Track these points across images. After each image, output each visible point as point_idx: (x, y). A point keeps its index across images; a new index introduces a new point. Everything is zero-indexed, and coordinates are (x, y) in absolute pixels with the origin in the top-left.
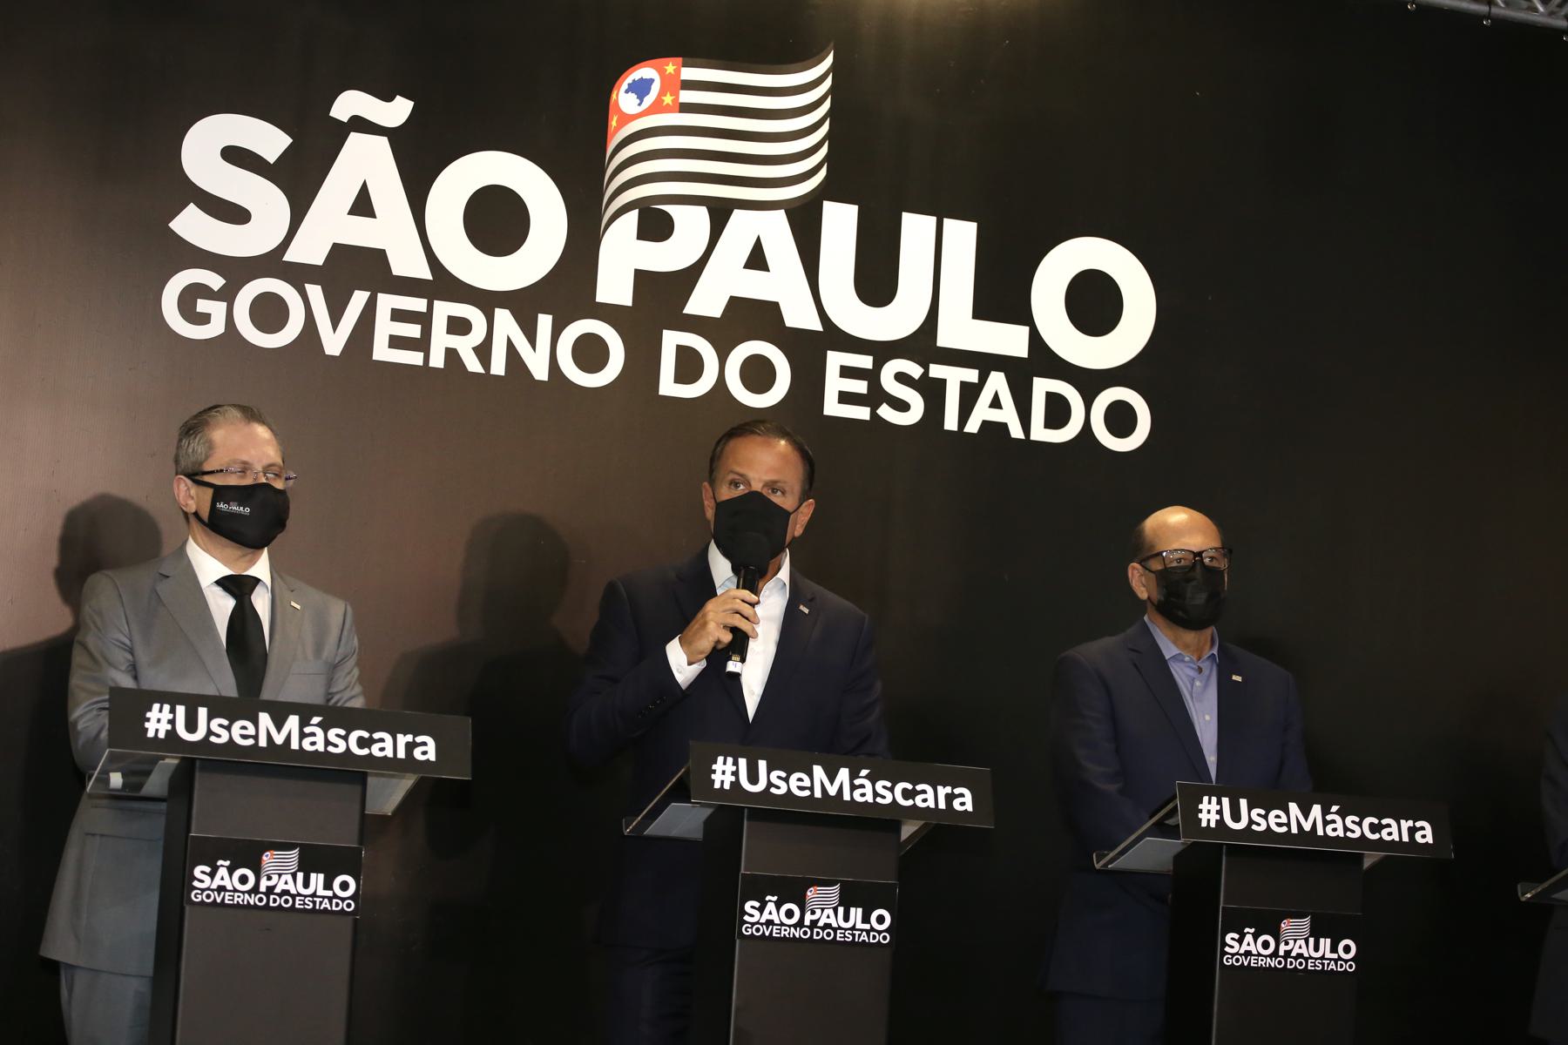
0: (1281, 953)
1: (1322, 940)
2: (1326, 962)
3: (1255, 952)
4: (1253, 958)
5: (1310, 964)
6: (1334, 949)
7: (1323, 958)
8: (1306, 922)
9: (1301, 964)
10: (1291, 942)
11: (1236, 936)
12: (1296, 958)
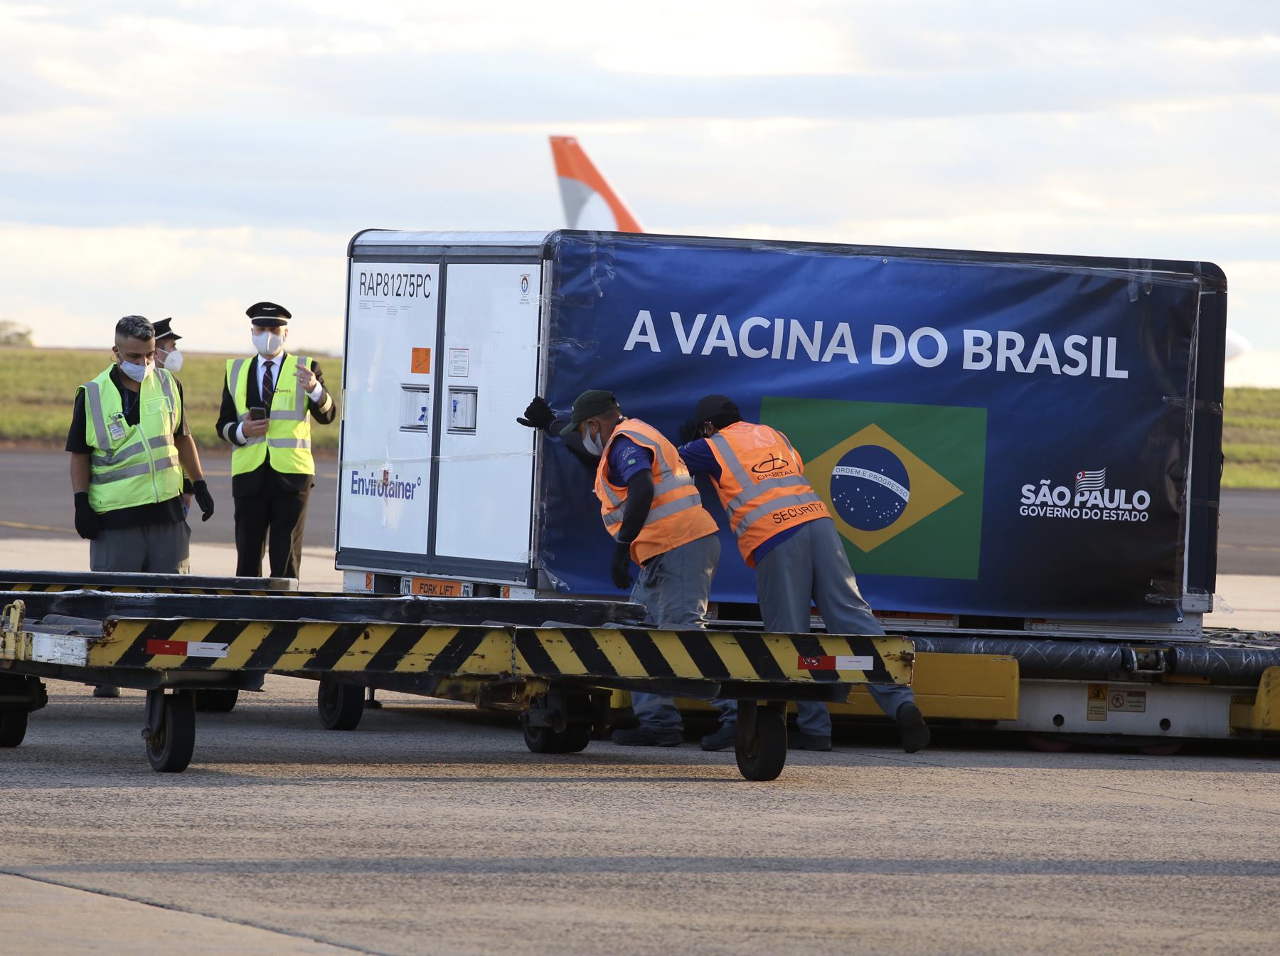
0: (1077, 504)
1: (1117, 491)
2: (1121, 512)
3: (1050, 503)
4: (1049, 508)
5: (1105, 515)
6: (1129, 500)
7: (1118, 508)
8: (1101, 473)
9: (1096, 514)
10: (1087, 494)
11: (1033, 488)
12: (1091, 509)
